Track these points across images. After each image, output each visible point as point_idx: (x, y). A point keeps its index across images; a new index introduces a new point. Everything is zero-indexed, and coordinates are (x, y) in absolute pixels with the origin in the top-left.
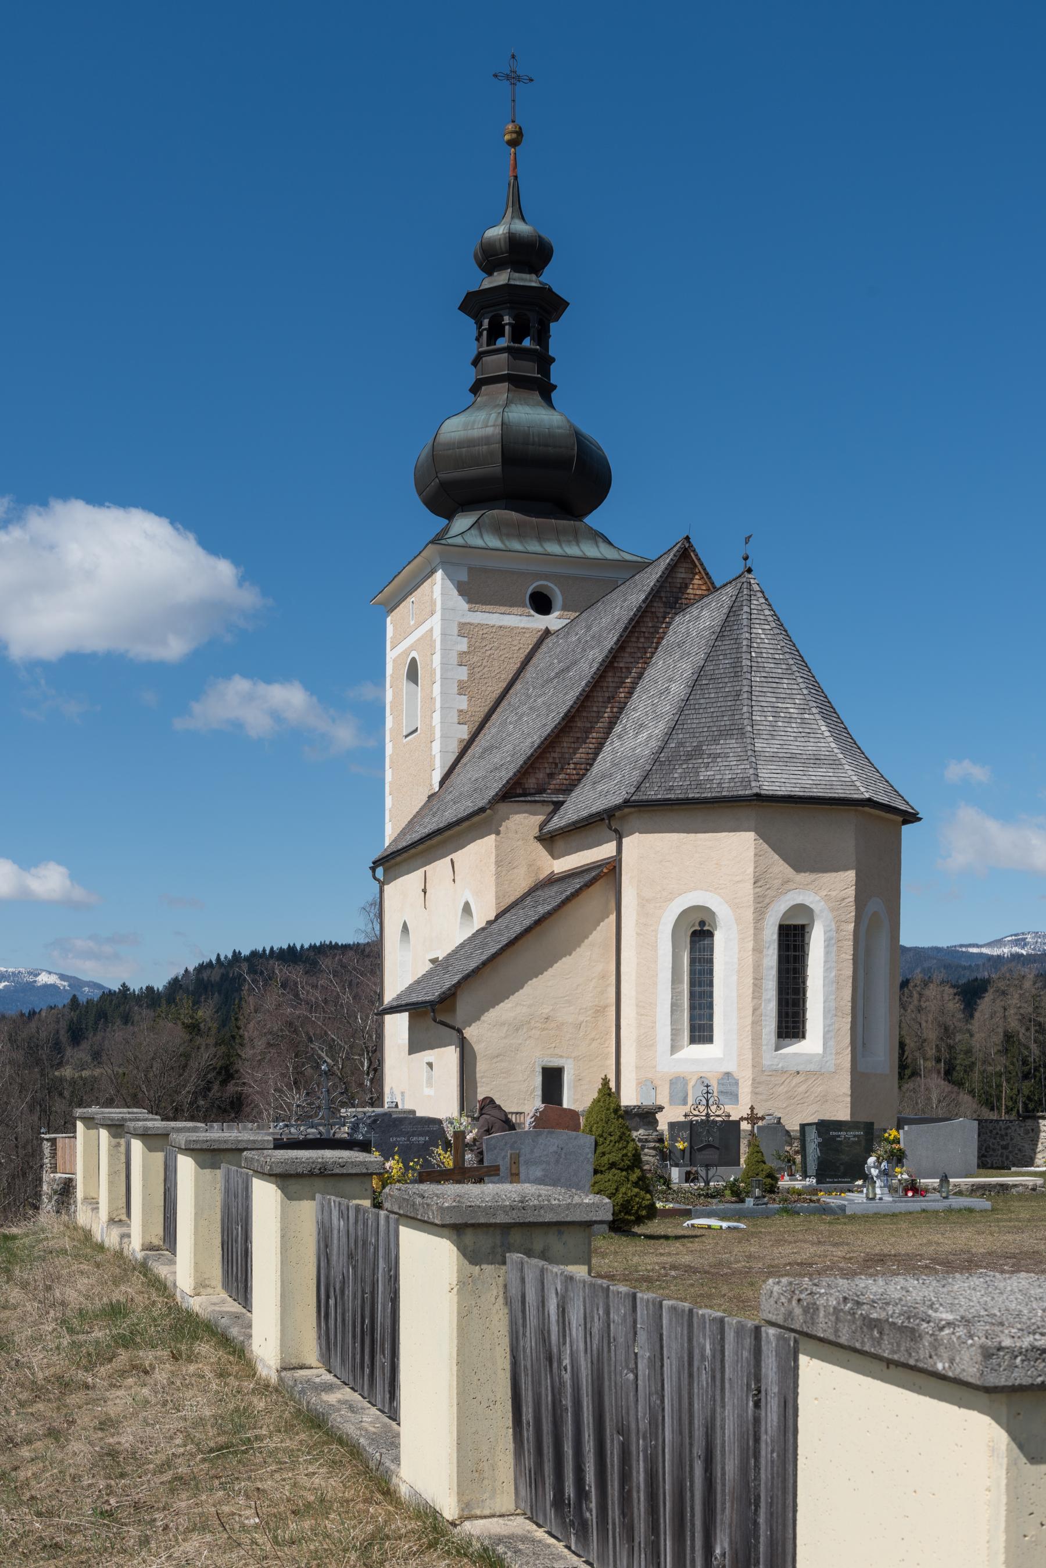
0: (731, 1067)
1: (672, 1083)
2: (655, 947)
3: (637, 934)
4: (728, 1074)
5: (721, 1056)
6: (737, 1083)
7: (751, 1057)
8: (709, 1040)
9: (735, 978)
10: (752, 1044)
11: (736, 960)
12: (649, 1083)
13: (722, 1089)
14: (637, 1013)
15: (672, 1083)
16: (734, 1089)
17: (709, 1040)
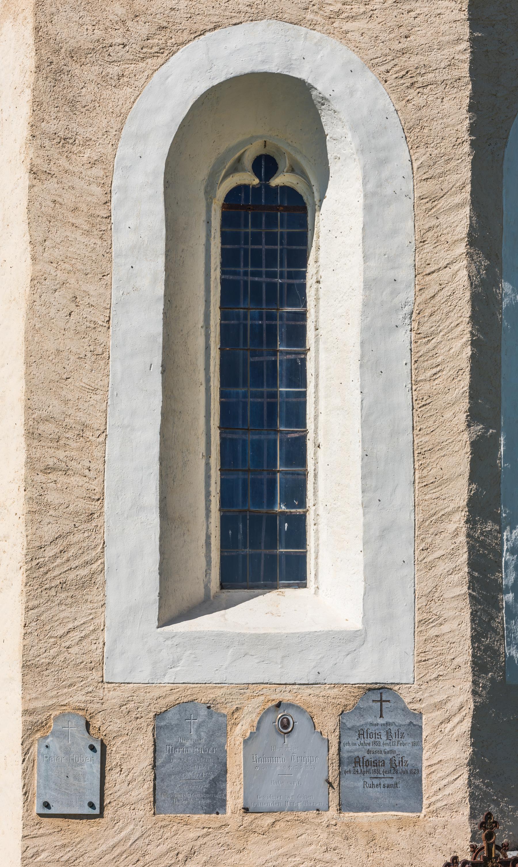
0: (389, 663)
1: (162, 724)
2: (101, 223)
3: (33, 172)
4: (380, 693)
5: (359, 626)
6: (414, 729)
7: (467, 630)
8: (295, 572)
9: (403, 337)
10: (473, 582)
11: (406, 274)
12: (75, 728)
13: (355, 747)
14: (31, 463)
15: (162, 724)
16: (403, 749)
17: (295, 572)
